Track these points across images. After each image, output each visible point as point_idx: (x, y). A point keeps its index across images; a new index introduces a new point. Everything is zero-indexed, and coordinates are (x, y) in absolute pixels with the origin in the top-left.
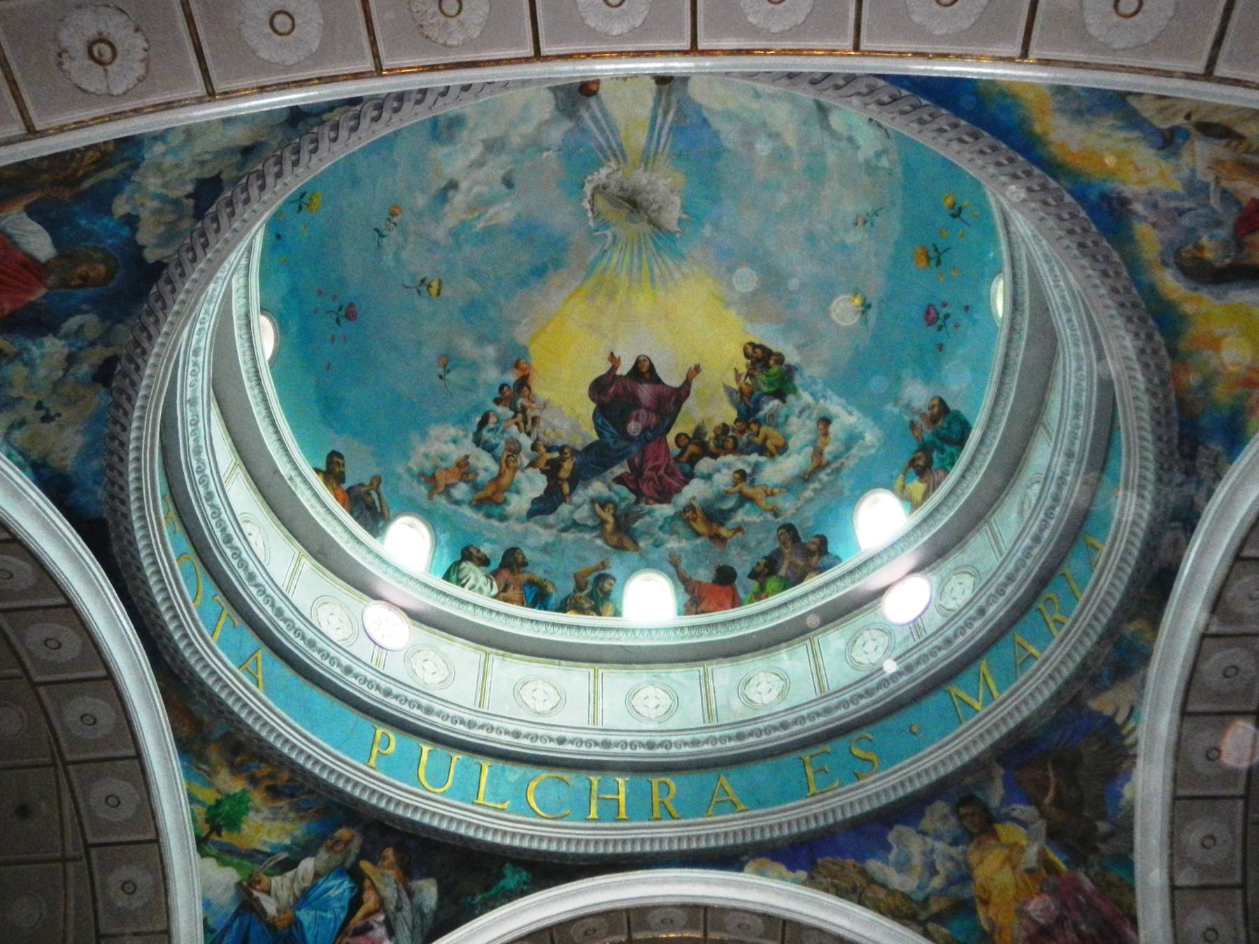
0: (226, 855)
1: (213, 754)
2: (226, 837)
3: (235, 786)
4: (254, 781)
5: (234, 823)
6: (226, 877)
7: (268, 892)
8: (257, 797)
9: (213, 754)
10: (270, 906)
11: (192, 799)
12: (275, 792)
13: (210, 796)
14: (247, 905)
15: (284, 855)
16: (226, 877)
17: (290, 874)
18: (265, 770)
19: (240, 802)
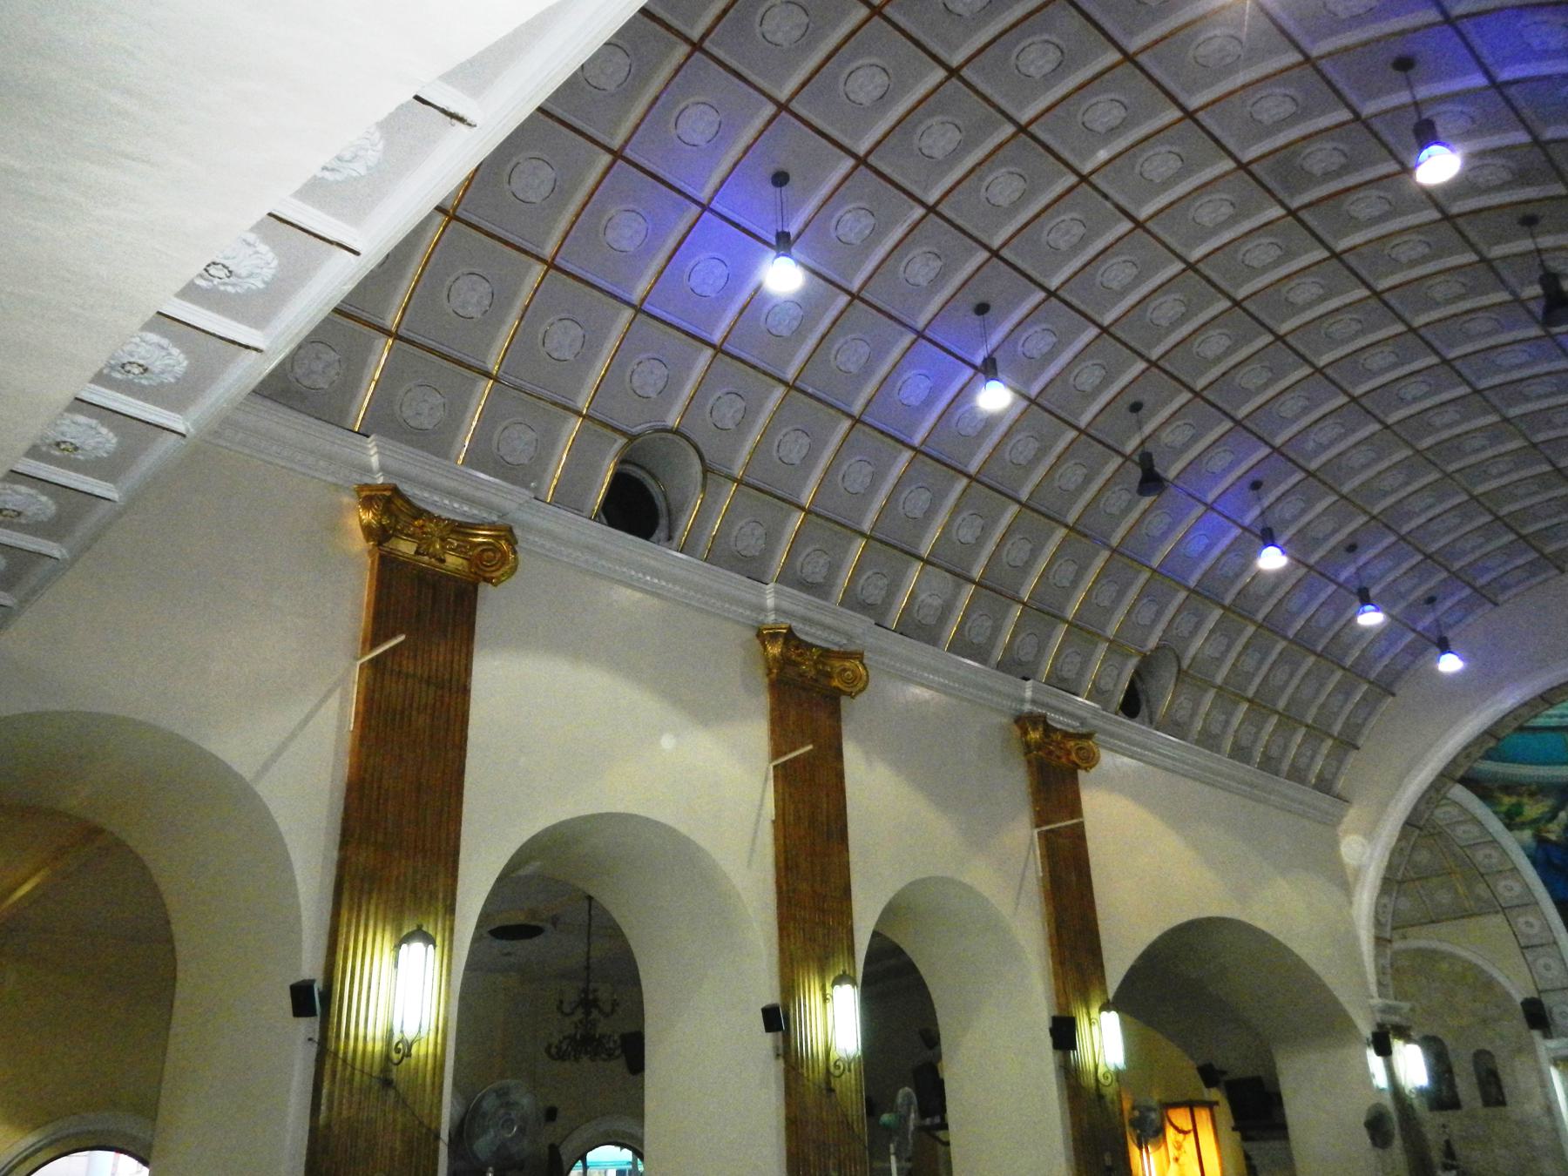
0: (1522, 826)
1: (1498, 794)
2: (1518, 820)
3: (1514, 800)
4: (1520, 795)
5: (1520, 814)
6: (1527, 835)
7: (1549, 832)
8: (1525, 800)
9: (1498, 794)
10: (1553, 837)
11: (1496, 813)
12: (1532, 794)
13: (1504, 809)
14: (1541, 841)
15: (1549, 815)
16: (1527, 835)
17: (1555, 822)
18: (1524, 788)
19: (1519, 805)
